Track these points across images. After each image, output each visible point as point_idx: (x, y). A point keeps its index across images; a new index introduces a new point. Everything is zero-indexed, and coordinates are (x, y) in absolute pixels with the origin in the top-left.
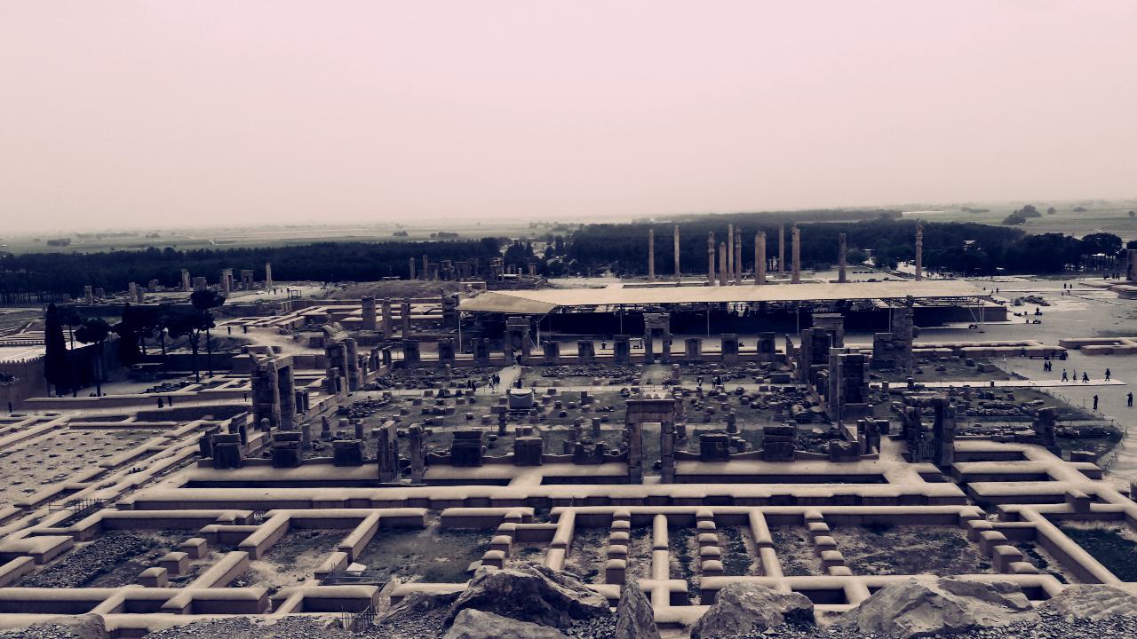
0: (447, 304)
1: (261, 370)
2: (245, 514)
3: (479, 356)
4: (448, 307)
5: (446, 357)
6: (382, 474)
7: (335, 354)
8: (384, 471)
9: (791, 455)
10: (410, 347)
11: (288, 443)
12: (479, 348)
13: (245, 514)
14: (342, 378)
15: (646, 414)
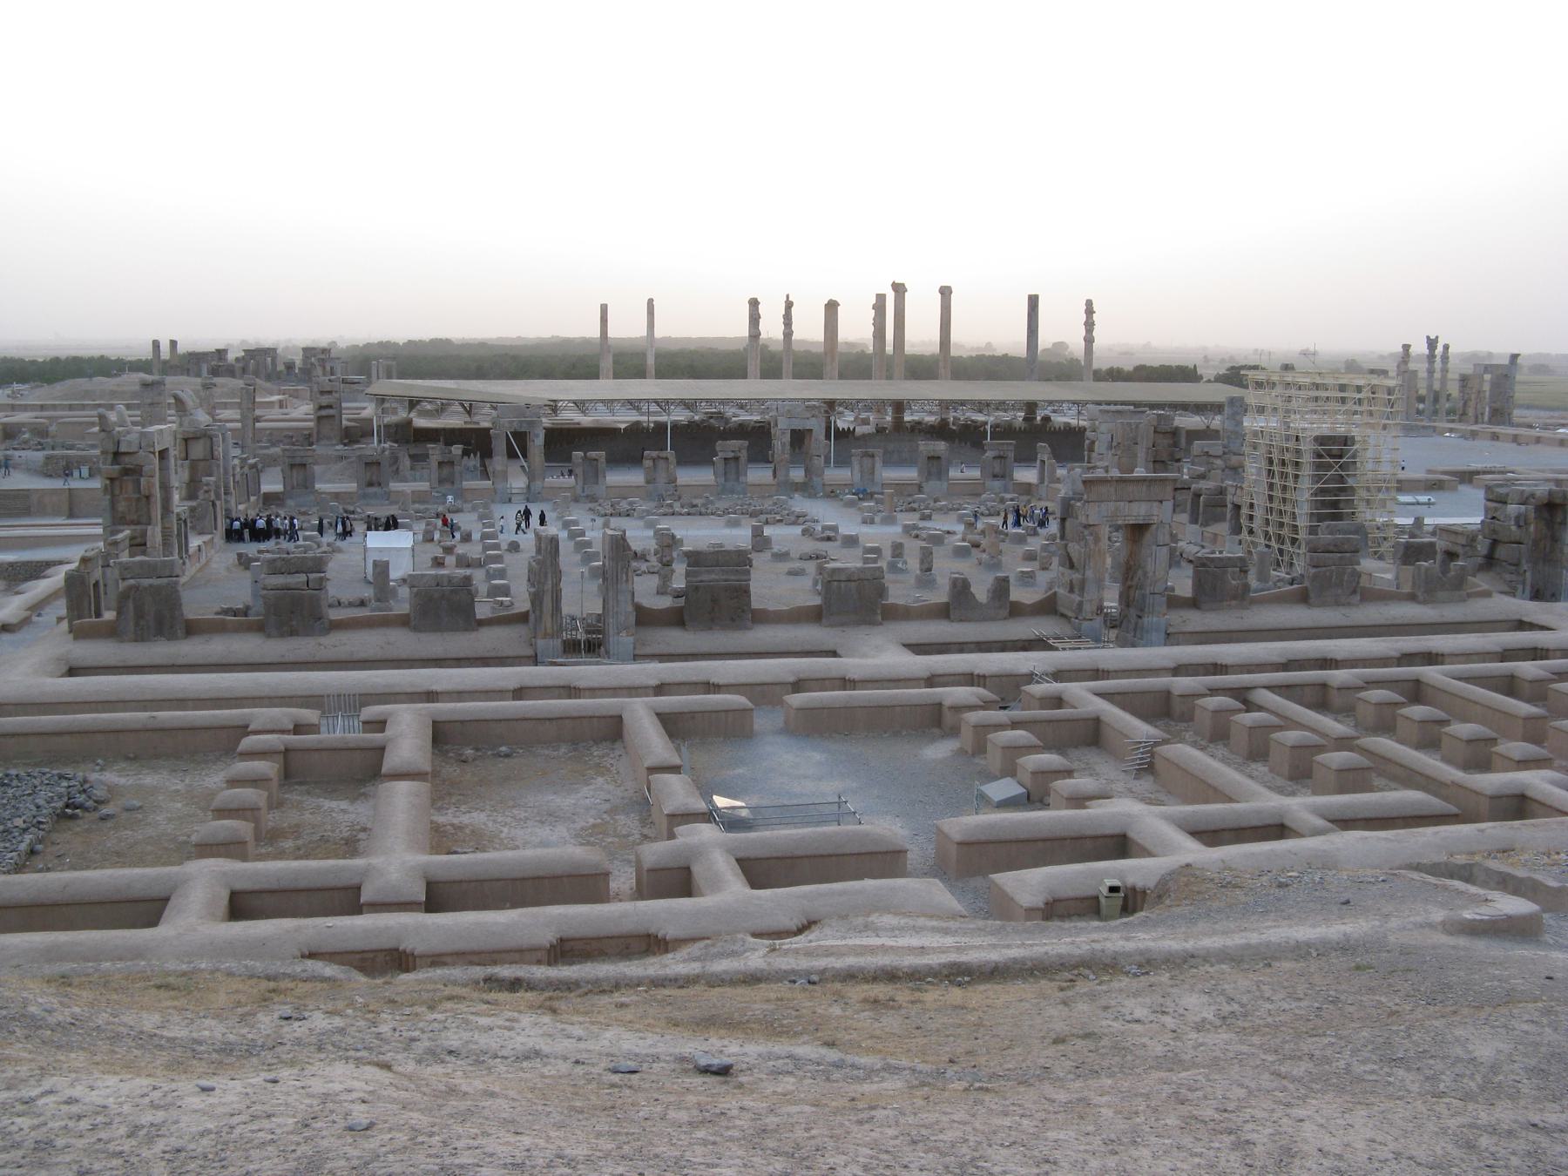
0: (322, 393)
1: (123, 449)
2: (309, 715)
3: (441, 481)
4: (325, 400)
5: (371, 484)
6: (541, 643)
7: (198, 450)
8: (545, 636)
9: (1354, 592)
10: (298, 461)
11: (302, 578)
12: (440, 464)
13: (309, 715)
14: (218, 503)
15: (1122, 504)
